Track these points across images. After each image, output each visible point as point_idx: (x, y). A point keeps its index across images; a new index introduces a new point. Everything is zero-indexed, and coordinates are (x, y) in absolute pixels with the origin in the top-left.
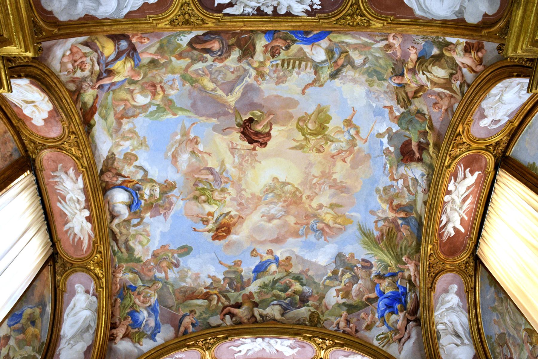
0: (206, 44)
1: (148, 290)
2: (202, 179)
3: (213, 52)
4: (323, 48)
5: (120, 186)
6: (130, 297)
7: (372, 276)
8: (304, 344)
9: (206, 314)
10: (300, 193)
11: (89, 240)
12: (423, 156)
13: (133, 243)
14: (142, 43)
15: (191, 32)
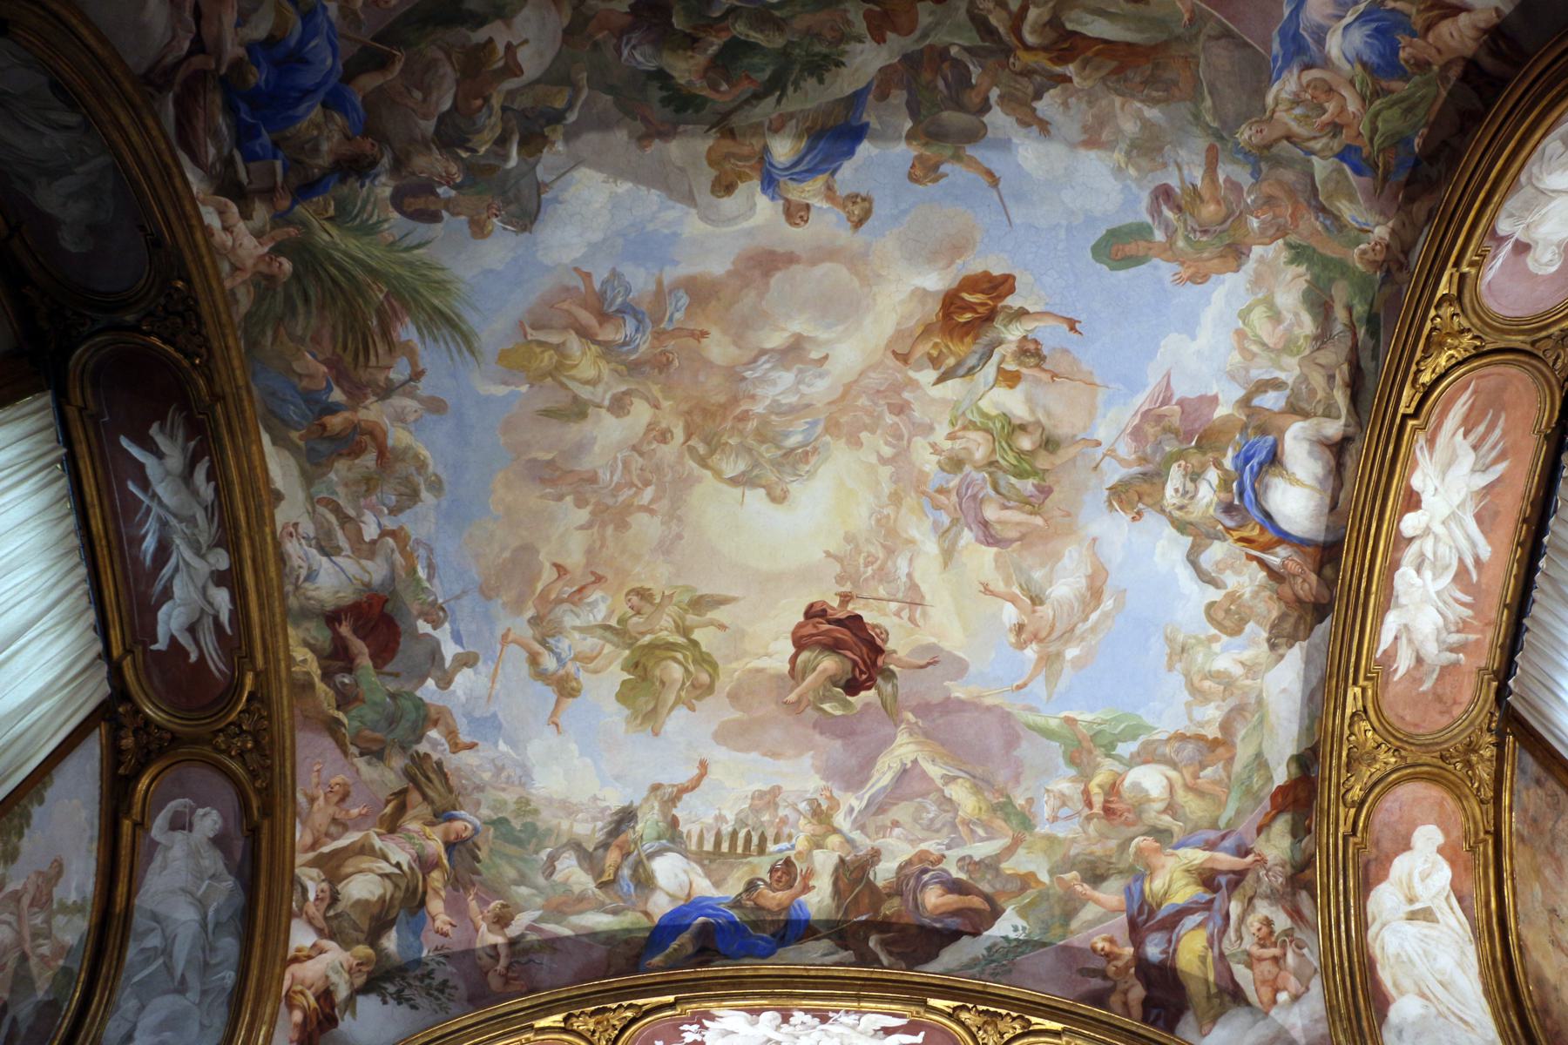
0: (955, 906)
1: (1295, 127)
3: (942, 883)
4: (661, 889)
5: (1284, 538)
6: (1374, 130)
7: (386, 161)
10: (692, 450)
12: (328, 633)
13: (1300, 325)
14: (1111, 941)
15: (989, 949)
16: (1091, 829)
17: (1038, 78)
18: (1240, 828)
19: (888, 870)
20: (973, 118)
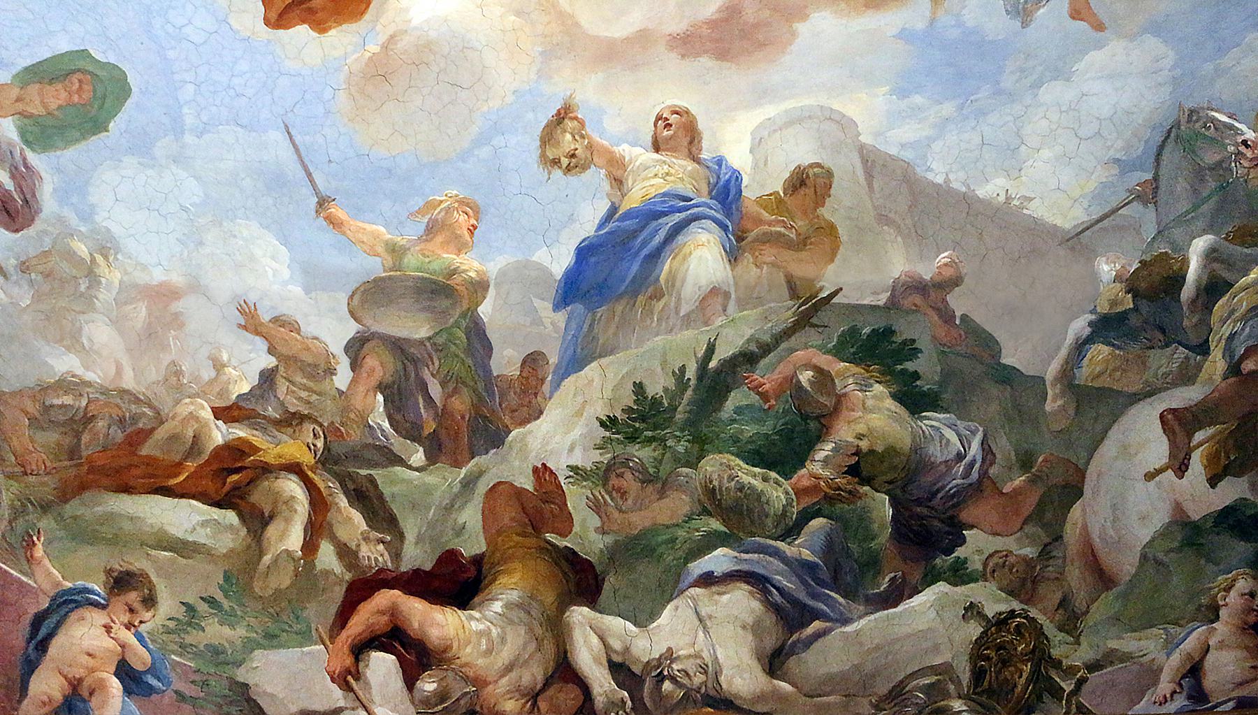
17: (272, 412)
20: (376, 328)
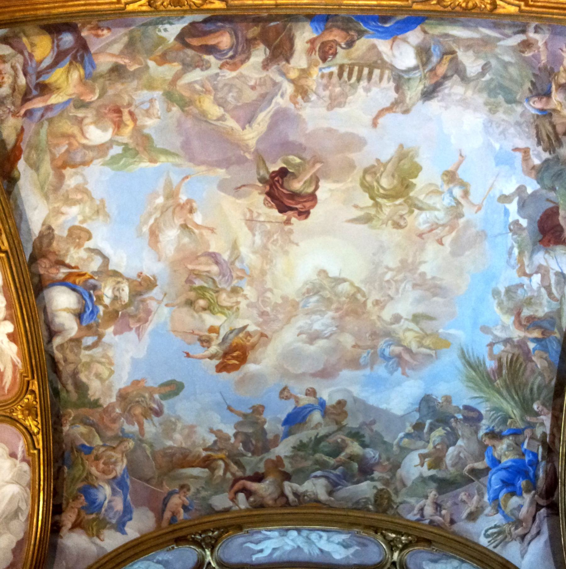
0: (208, 37)
1: (113, 453)
2: (199, 271)
3: (220, 51)
4: (413, 47)
5: (62, 282)
6: (83, 464)
7: (481, 433)
8: (365, 541)
9: (206, 490)
11: (14, 372)
16: (126, 99)
18: (33, 126)
19: (257, 56)
20: (240, 430)
